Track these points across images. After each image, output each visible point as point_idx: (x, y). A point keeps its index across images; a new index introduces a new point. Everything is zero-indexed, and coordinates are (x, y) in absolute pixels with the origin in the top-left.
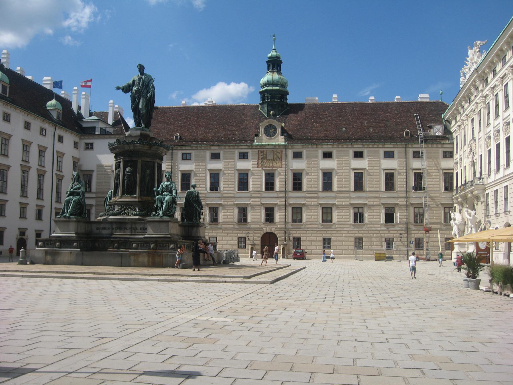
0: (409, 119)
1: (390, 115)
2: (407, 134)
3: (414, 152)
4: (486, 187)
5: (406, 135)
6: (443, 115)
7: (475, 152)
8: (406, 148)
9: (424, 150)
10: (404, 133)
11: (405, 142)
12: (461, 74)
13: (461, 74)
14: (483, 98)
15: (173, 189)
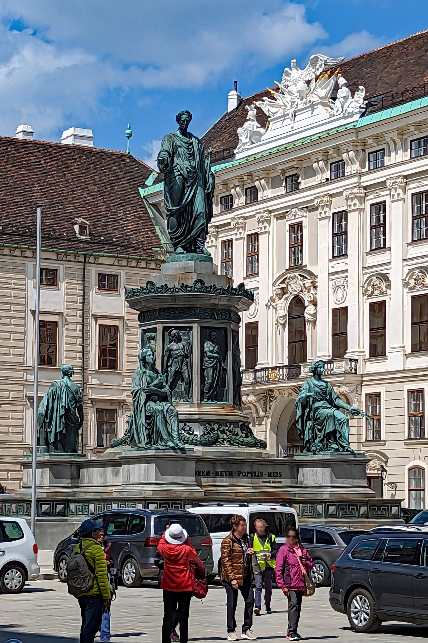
0: (73, 191)
1: (29, 176)
2: (83, 228)
3: (101, 277)
4: (364, 379)
5: (81, 233)
6: (143, 192)
7: (306, 298)
8: (85, 263)
9: (122, 273)
10: (77, 228)
11: (83, 250)
12: (250, 113)
13: (252, 113)
14: (362, 190)
15: (334, 396)
